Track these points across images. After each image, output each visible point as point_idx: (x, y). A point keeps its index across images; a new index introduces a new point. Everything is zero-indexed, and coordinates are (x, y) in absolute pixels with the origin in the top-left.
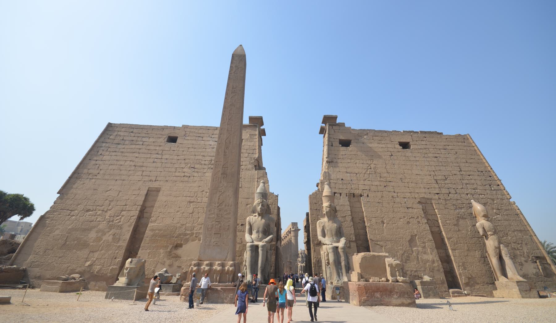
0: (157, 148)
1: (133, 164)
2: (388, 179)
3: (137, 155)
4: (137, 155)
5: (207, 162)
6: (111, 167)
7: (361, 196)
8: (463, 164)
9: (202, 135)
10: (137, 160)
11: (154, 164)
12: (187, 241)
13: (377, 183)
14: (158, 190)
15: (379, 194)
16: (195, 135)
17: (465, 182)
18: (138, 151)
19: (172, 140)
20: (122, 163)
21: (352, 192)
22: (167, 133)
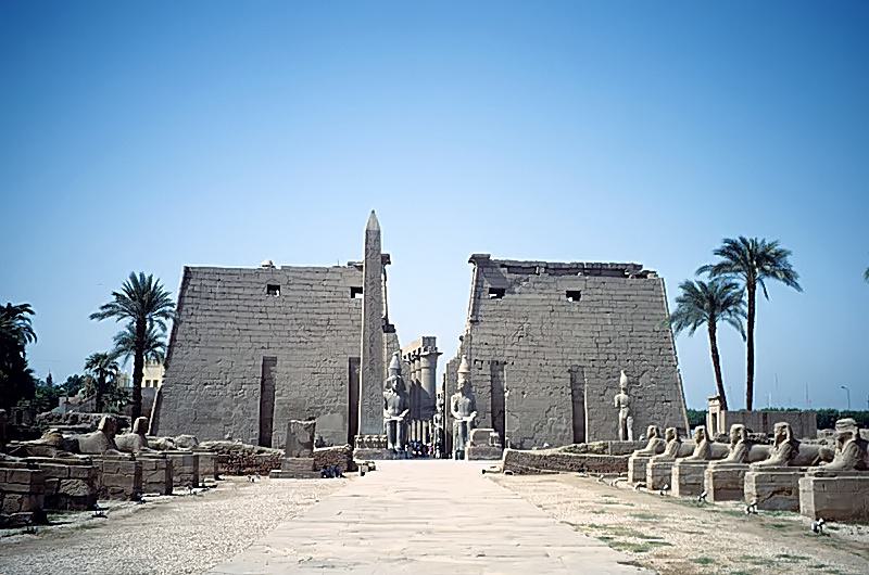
0: (259, 304)
1: (236, 327)
2: (541, 343)
3: (236, 314)
4: (236, 314)
5: (324, 323)
6: (210, 332)
7: (505, 363)
8: (638, 322)
9: (311, 282)
10: (238, 321)
11: (261, 327)
12: (319, 414)
13: (527, 349)
14: (274, 360)
15: (526, 361)
16: (302, 281)
17: (630, 345)
18: (235, 308)
19: (272, 289)
20: (223, 326)
21: (496, 359)
22: (264, 278)
